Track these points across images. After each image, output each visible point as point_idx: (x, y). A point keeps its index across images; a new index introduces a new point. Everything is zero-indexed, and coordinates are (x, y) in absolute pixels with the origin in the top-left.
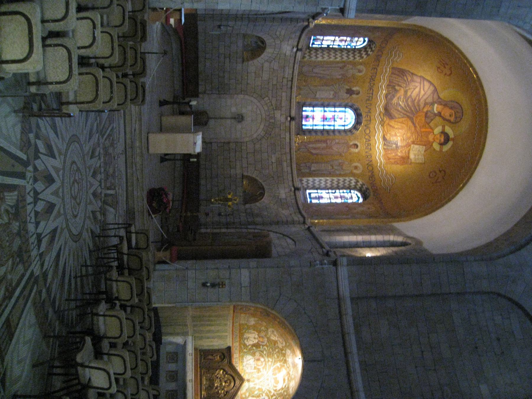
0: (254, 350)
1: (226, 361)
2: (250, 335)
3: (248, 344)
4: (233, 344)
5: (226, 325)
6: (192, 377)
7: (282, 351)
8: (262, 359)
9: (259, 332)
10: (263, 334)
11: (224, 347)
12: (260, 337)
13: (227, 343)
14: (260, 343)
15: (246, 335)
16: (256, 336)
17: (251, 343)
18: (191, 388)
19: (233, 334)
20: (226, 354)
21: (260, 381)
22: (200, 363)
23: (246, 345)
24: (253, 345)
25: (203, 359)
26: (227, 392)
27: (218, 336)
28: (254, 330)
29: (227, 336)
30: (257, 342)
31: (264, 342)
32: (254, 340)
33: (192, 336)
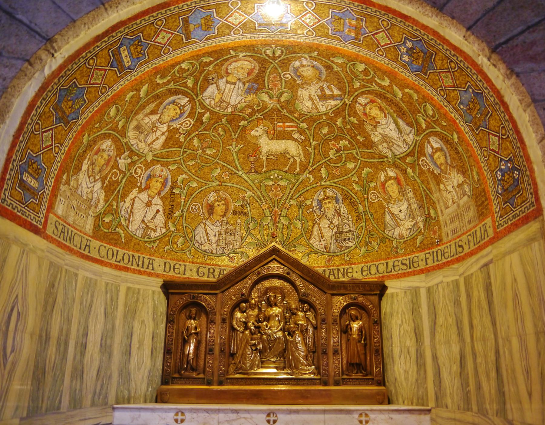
0: (182, 216)
1: (208, 300)
2: (138, 216)
3: (164, 231)
4: (158, 276)
5: (90, 285)
6: (261, 411)
7: (202, 123)
8: (212, 197)
9: (132, 183)
10: (141, 173)
11: (161, 301)
12: (148, 188)
13: (154, 292)
14: (163, 193)
15: (135, 226)
16: (144, 196)
17: (160, 219)
18: (294, 416)
19: (126, 269)
20: (185, 299)
21: (267, 212)
22: (209, 383)
23: (165, 236)
24: (169, 214)
25: (194, 374)
26: (302, 301)
27: (125, 316)
28: (124, 197)
29: (128, 289)
30: (162, 199)
31: (166, 179)
32: (154, 209)
33: (114, 409)
